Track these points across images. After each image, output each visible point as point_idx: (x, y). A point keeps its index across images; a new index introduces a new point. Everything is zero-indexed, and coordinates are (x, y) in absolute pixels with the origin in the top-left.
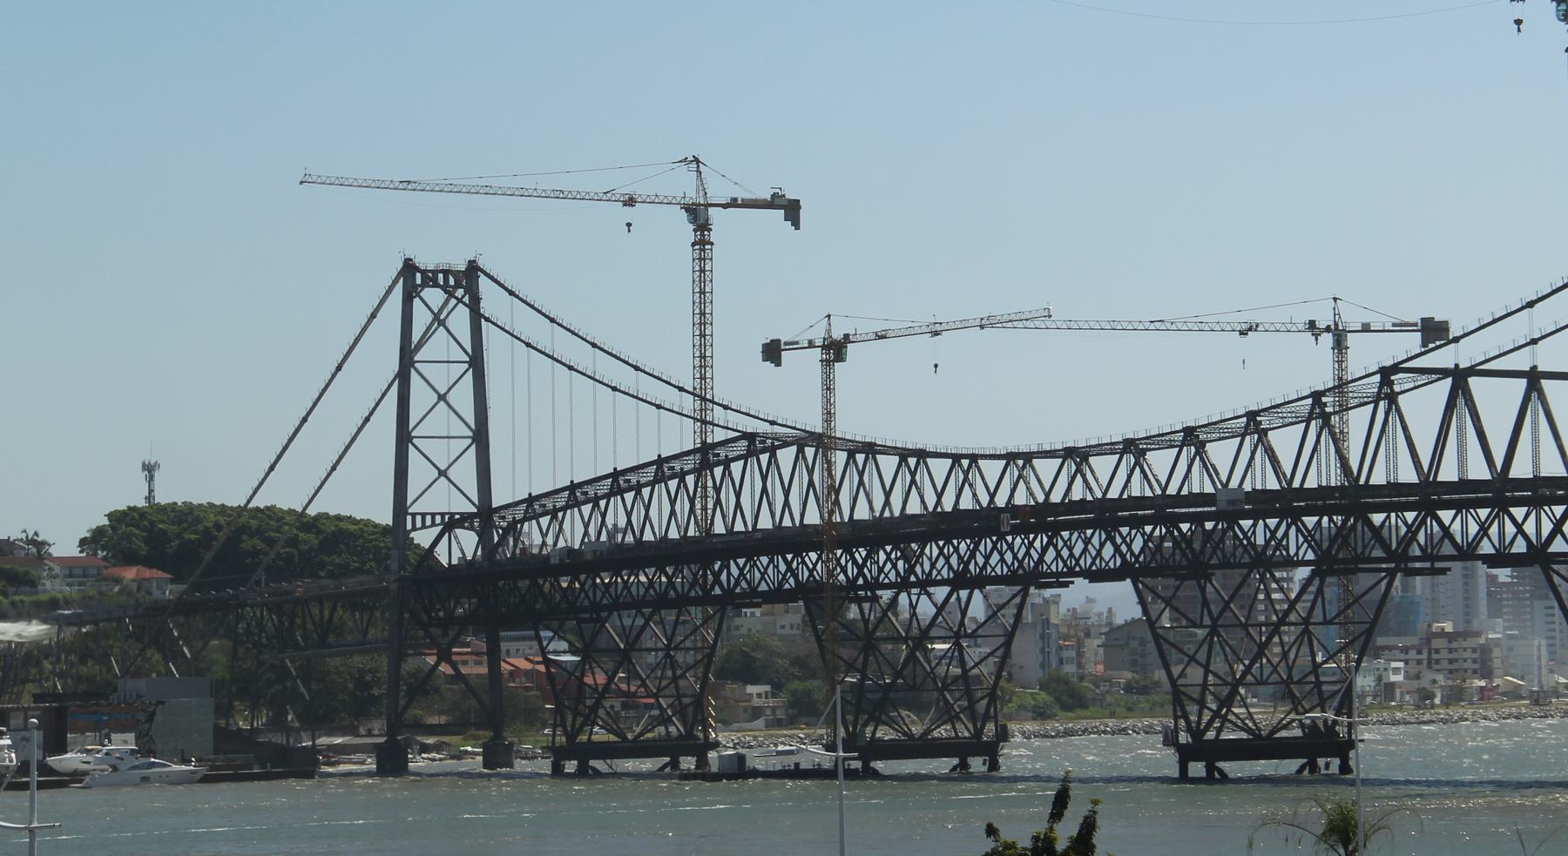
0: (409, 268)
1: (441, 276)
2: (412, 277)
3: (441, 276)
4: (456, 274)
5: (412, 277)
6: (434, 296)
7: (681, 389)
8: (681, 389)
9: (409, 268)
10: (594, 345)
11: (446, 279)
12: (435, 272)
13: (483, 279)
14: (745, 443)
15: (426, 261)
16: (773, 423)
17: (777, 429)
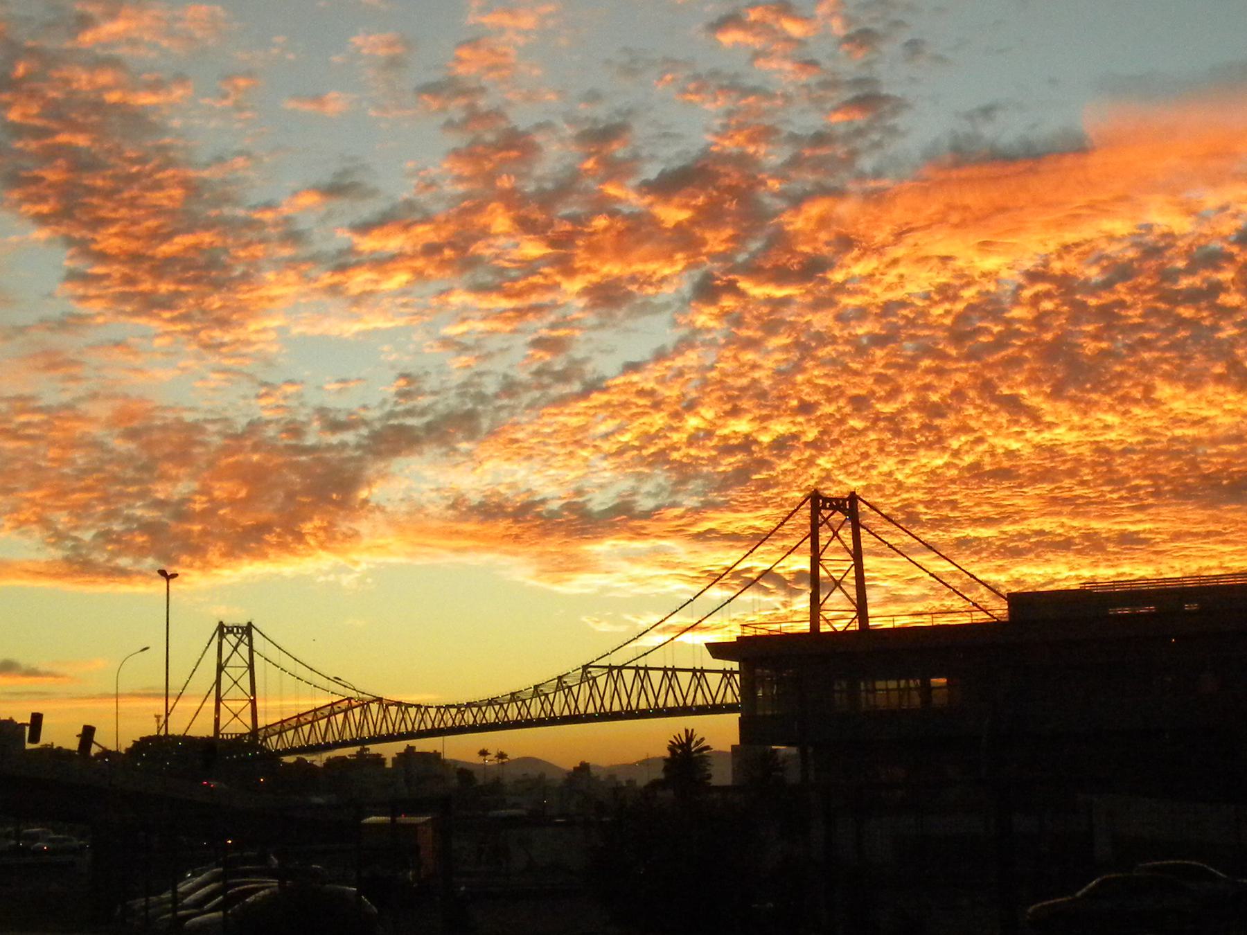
0: (221, 626)
1: (235, 629)
2: (223, 630)
3: (235, 629)
4: (242, 628)
5: (223, 630)
6: (230, 637)
7: (329, 679)
8: (329, 679)
9: (221, 626)
10: (295, 659)
11: (238, 630)
12: (233, 628)
13: (254, 630)
14: (347, 701)
15: (227, 622)
16: (363, 693)
17: (365, 696)
